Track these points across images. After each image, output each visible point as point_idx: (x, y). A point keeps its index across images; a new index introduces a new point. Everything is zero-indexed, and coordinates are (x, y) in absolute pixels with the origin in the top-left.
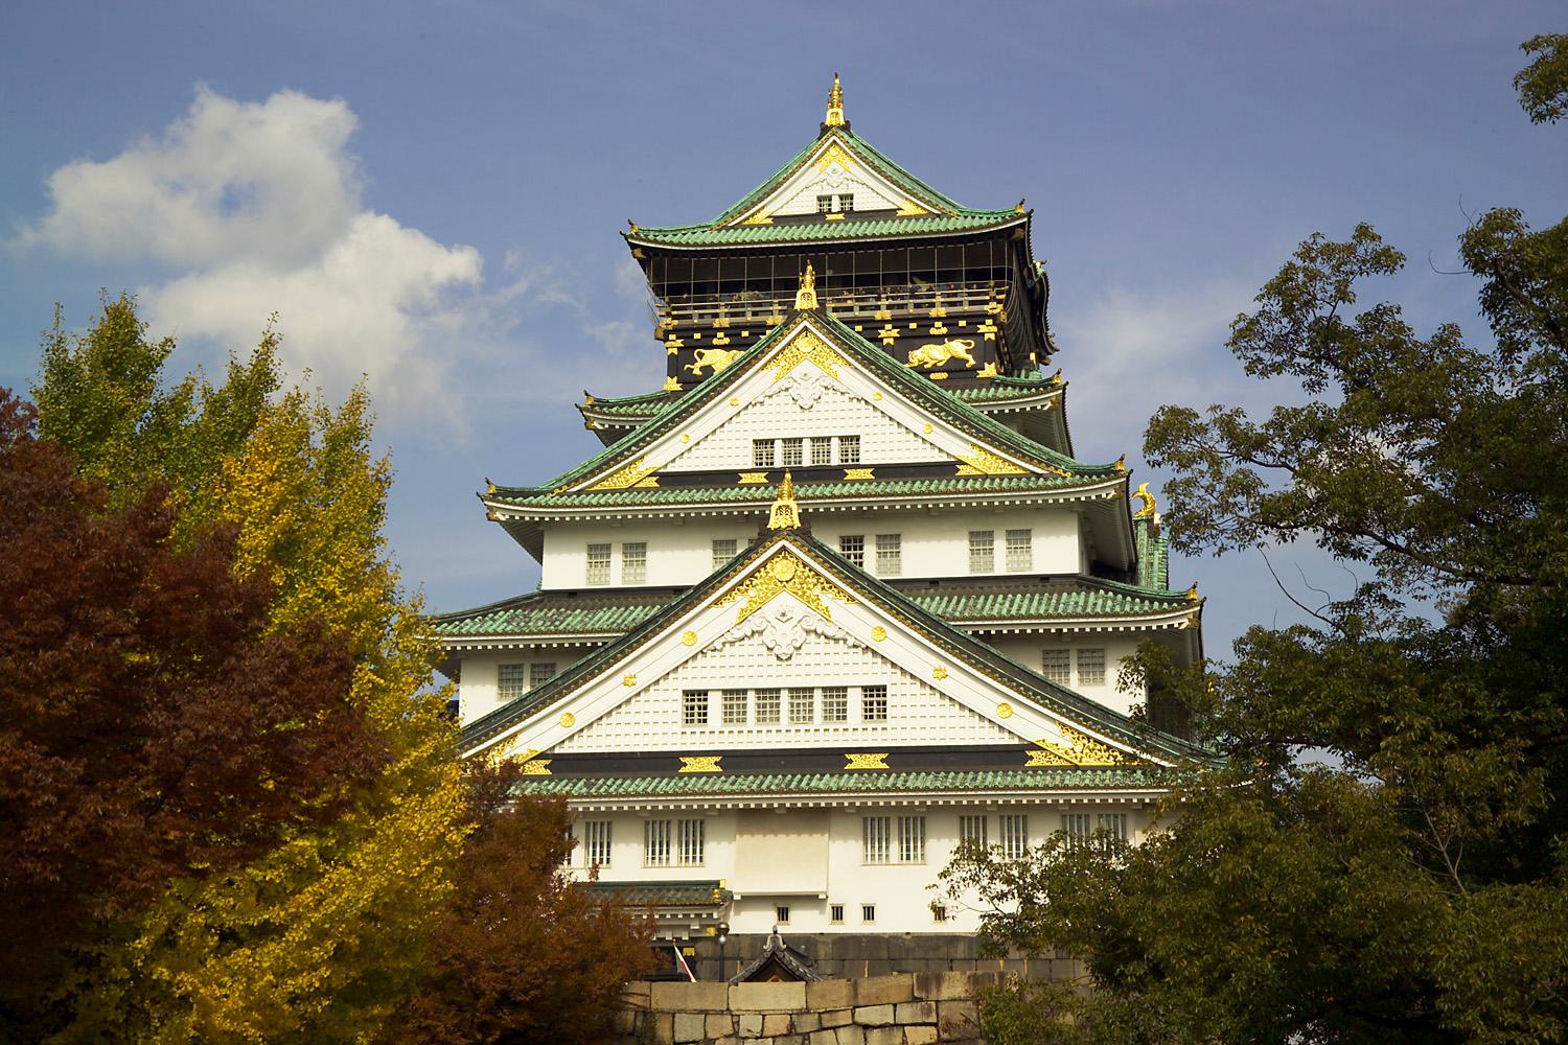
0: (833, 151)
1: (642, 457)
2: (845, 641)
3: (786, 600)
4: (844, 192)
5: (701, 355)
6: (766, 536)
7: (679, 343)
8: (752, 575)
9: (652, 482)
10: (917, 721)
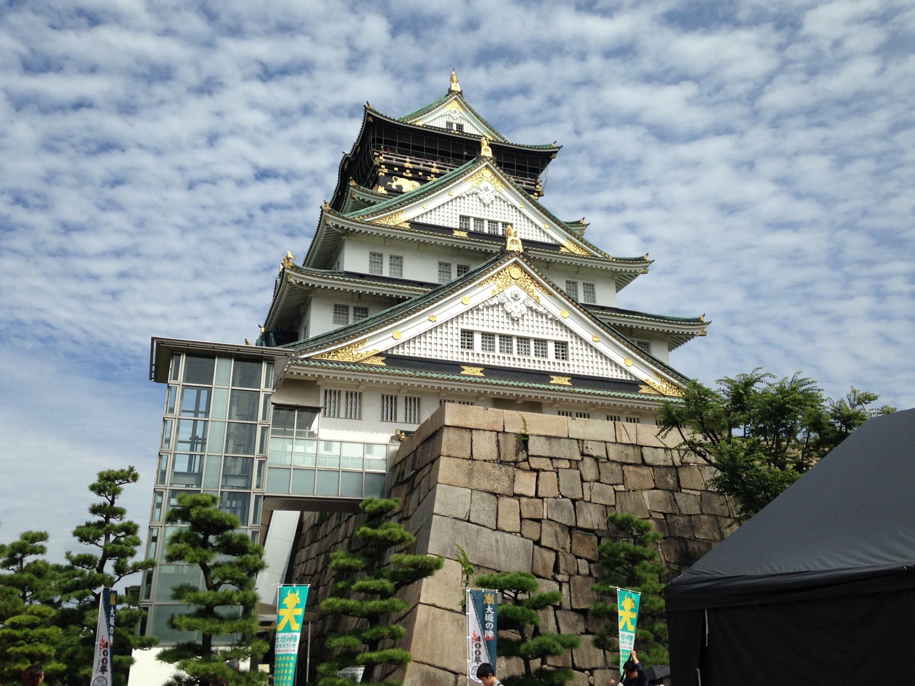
0: (455, 103)
1: (402, 211)
2: (546, 316)
3: (514, 289)
4: (458, 122)
5: (396, 180)
6: (504, 253)
7: (386, 171)
8: (498, 273)
9: (407, 226)
10: (582, 363)
